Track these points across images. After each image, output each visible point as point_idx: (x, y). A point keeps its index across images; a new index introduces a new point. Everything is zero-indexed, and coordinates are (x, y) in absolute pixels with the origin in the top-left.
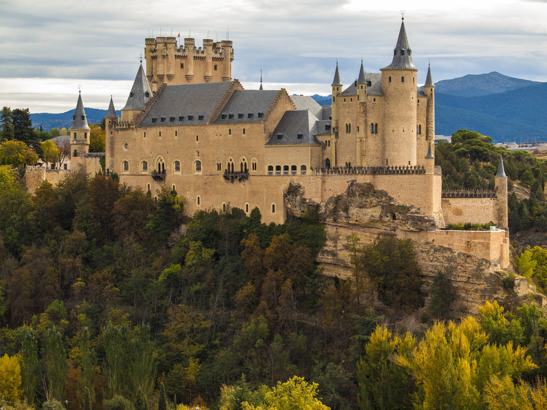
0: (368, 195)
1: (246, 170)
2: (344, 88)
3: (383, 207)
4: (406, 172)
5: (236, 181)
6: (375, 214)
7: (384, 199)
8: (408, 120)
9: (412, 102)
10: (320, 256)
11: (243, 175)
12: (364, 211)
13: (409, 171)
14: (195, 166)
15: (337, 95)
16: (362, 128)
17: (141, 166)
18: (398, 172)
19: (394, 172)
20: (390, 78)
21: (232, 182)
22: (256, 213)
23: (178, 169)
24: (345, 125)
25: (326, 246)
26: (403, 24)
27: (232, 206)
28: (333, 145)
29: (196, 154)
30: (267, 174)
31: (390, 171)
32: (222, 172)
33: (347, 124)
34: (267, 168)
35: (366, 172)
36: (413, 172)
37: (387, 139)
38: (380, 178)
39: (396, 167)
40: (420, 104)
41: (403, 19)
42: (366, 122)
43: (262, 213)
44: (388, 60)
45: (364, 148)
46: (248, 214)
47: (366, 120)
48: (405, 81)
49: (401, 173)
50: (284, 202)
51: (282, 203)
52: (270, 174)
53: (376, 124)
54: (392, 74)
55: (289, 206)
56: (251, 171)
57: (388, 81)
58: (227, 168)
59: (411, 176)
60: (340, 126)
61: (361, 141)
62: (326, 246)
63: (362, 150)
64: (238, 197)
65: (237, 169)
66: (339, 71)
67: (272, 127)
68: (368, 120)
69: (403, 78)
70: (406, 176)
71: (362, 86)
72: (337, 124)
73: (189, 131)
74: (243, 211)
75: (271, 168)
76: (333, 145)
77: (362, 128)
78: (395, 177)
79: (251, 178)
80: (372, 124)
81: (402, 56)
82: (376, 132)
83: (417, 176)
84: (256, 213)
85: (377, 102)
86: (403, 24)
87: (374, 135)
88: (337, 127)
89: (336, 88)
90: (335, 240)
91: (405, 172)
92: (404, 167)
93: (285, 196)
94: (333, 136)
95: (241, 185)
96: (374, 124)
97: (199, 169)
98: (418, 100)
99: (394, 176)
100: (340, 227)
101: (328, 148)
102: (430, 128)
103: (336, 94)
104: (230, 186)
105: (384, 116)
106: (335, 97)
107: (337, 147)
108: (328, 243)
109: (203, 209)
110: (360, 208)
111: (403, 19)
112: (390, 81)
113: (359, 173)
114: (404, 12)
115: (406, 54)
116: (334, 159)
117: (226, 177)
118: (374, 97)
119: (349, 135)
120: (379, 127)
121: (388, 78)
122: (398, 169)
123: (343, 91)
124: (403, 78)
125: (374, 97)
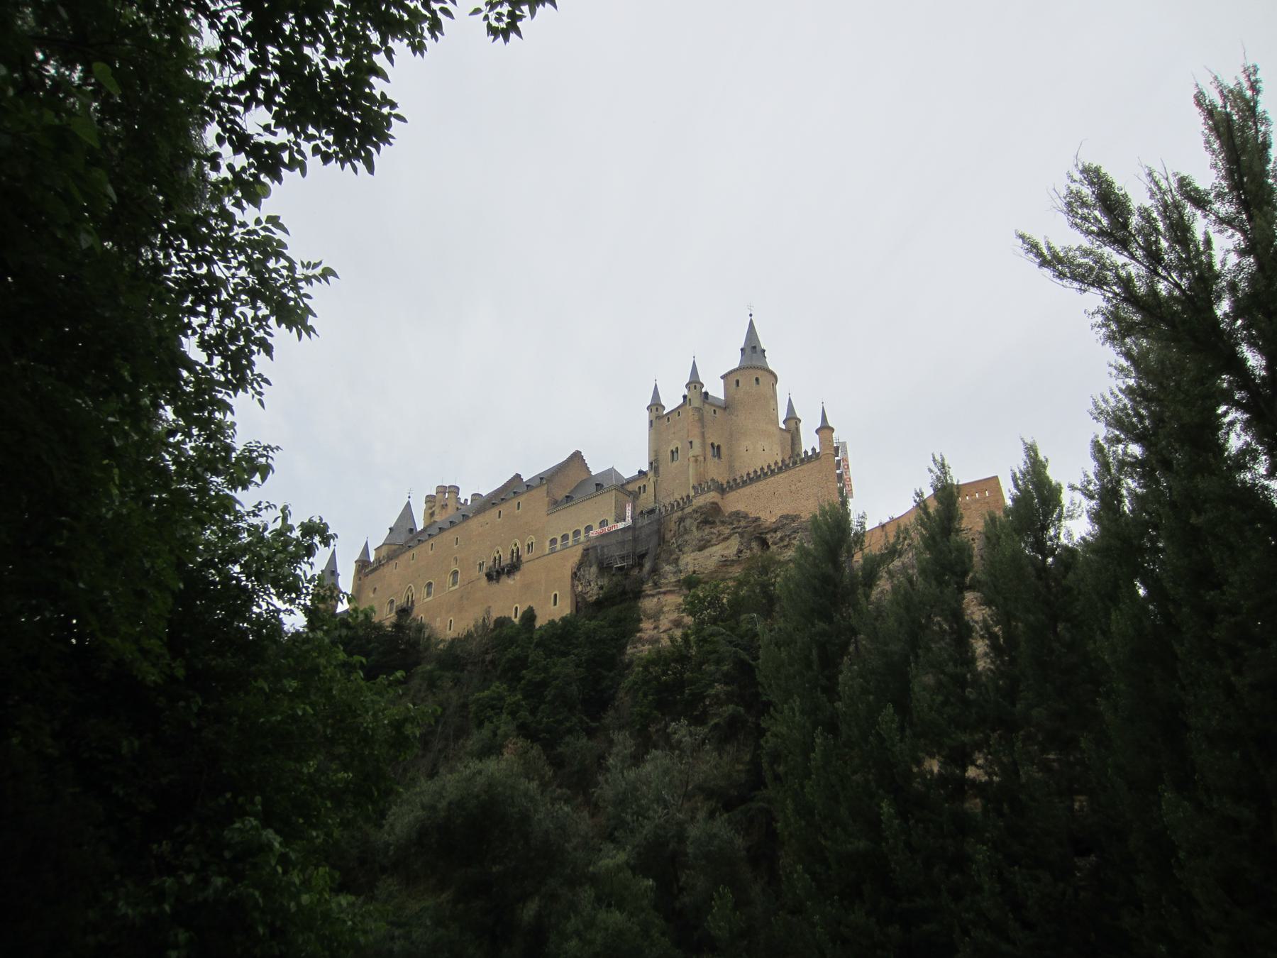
0: (714, 522)
1: (518, 557)
3: (741, 535)
5: (504, 578)
6: (726, 552)
7: (743, 523)
10: (629, 650)
11: (514, 568)
12: (706, 552)
14: (450, 579)
17: (387, 608)
21: (498, 580)
22: (529, 616)
23: (429, 594)
25: (640, 630)
27: (495, 615)
28: (650, 489)
29: (453, 562)
30: (547, 551)
32: (485, 571)
34: (548, 543)
35: (709, 488)
38: (732, 496)
42: (703, 434)
43: (538, 612)
46: (516, 621)
50: (573, 586)
51: (569, 588)
52: (553, 551)
53: (719, 447)
55: (580, 588)
56: (525, 556)
58: (491, 564)
62: (640, 630)
64: (507, 602)
65: (506, 560)
67: (561, 494)
73: (449, 536)
74: (510, 619)
75: (553, 541)
76: (650, 489)
77: (697, 442)
78: (761, 485)
79: (524, 567)
80: (712, 445)
82: (719, 457)
84: (529, 616)
85: (717, 415)
90: (656, 616)
93: (574, 575)
95: (511, 582)
97: (454, 583)
100: (665, 593)
101: (643, 496)
104: (495, 587)
105: (731, 435)
108: (646, 625)
109: (455, 635)
110: (701, 549)
117: (489, 577)
119: (675, 463)
120: (723, 450)
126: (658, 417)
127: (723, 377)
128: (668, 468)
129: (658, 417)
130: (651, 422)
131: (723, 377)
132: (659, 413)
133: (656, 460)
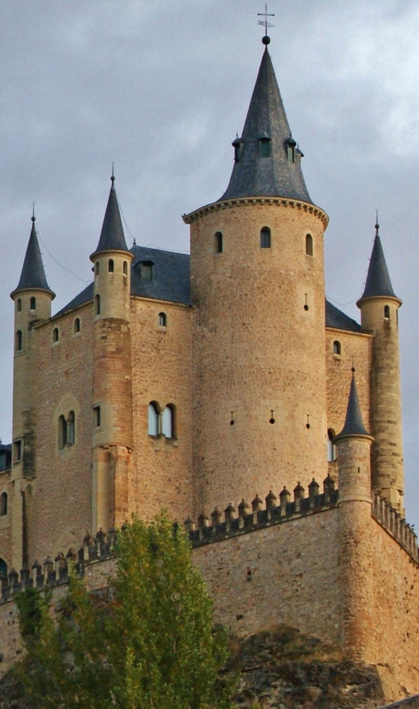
2: (56, 307)
4: (271, 515)
8: (290, 382)
9: (303, 320)
13: (276, 512)
15: (31, 324)
16: (112, 410)
18: (235, 524)
19: (221, 528)
20: (219, 236)
24: (56, 423)
26: (266, 58)
31: (207, 532)
33: (62, 417)
36: (291, 508)
37: (210, 456)
39: (229, 510)
40: (343, 356)
41: (266, 41)
44: (213, 179)
45: (119, 481)
47: (128, 384)
48: (274, 243)
49: (250, 527)
54: (228, 221)
57: (211, 249)
59: (283, 527)
60: (38, 431)
61: (110, 458)
63: (111, 491)
66: (39, 237)
68: (137, 386)
69: (266, 231)
70: (267, 533)
71: (111, 263)
72: (29, 424)
80: (154, 404)
81: (263, 162)
83: (311, 521)
86: (266, 58)
87: (161, 444)
88: (29, 437)
89: (26, 298)
91: (262, 516)
92: (256, 502)
94: (17, 471)
96: (162, 405)
98: (337, 344)
99: (223, 544)
102: (384, 446)
103: (27, 320)
105: (200, 377)
106: (25, 332)
107: (30, 511)
111: (266, 41)
112: (220, 249)
113: (93, 555)
114: (270, 20)
115: (278, 154)
116: (18, 551)
118: (162, 309)
119: (69, 453)
121: (213, 240)
122: (235, 515)
123: (53, 314)
124: (266, 231)
125: (162, 309)
126: (35, 324)
127: (189, 219)
128: (53, 460)
129: (35, 324)
130: (19, 334)
131: (189, 219)
132: (39, 312)
133: (29, 437)
